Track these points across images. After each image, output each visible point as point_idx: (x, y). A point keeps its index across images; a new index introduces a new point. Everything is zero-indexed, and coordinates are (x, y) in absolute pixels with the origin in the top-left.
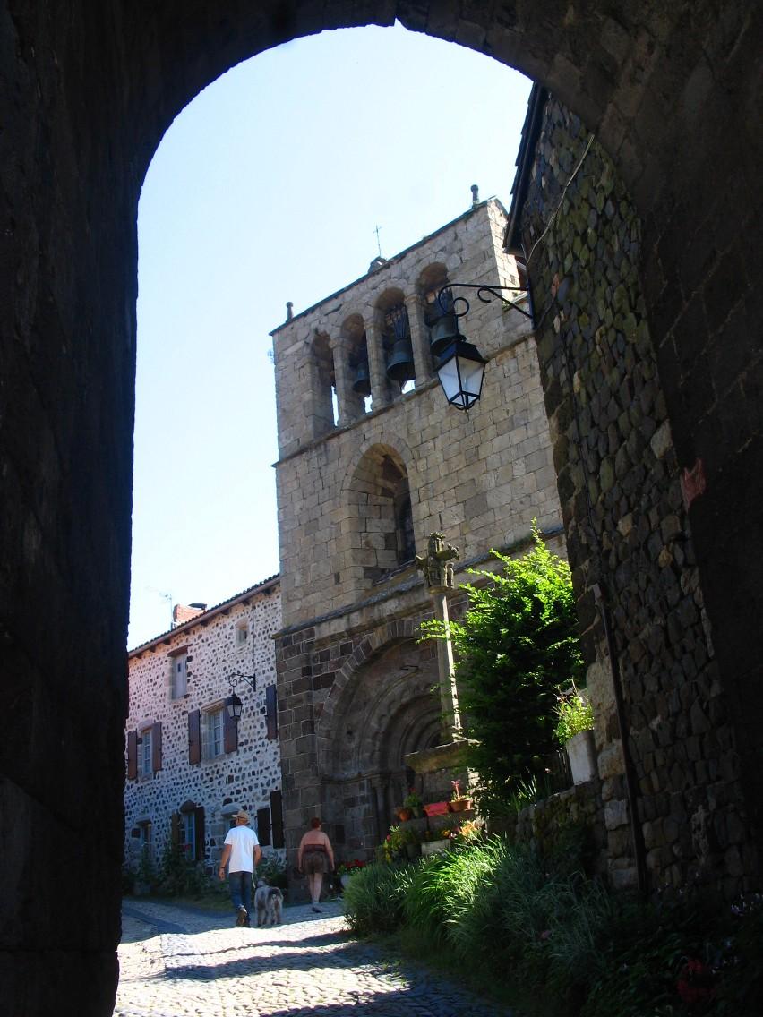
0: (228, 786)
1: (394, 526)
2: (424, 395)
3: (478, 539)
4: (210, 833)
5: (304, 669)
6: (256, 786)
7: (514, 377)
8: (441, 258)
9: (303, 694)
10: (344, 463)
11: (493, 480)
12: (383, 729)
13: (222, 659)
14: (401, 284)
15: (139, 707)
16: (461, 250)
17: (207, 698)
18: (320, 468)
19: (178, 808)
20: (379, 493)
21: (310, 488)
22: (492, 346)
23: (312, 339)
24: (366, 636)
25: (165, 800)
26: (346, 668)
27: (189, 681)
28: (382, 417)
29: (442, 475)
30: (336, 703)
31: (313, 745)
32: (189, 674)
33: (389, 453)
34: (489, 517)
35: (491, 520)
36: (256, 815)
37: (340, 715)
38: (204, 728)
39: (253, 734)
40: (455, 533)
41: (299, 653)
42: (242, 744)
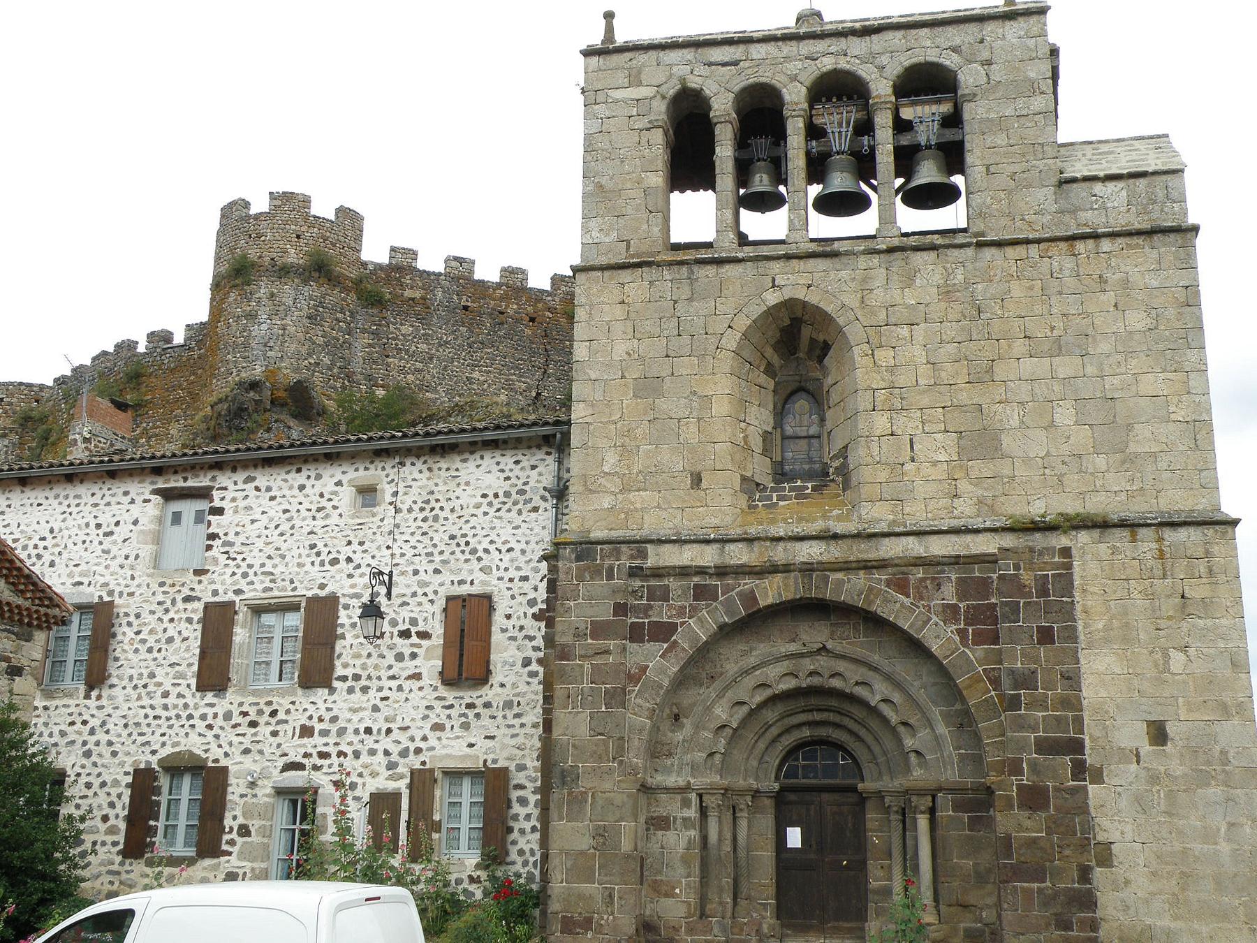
0: (297, 741)
2: (897, 255)
3: (980, 492)
4: (238, 812)
6: (372, 752)
7: (1071, 283)
9: (612, 644)
11: (1016, 417)
12: (735, 725)
13: (309, 529)
14: (865, 71)
15: (52, 564)
16: (989, 63)
17: (259, 587)
18: (676, 302)
19: (154, 760)
22: (1030, 224)
23: (672, 92)
24: (748, 583)
25: (114, 739)
26: (701, 621)
27: (209, 548)
28: (812, 262)
30: (675, 669)
32: (213, 537)
33: (806, 317)
35: (1006, 471)
36: (366, 798)
38: (240, 635)
39: (376, 667)
40: (940, 473)
41: (610, 576)
42: (344, 679)
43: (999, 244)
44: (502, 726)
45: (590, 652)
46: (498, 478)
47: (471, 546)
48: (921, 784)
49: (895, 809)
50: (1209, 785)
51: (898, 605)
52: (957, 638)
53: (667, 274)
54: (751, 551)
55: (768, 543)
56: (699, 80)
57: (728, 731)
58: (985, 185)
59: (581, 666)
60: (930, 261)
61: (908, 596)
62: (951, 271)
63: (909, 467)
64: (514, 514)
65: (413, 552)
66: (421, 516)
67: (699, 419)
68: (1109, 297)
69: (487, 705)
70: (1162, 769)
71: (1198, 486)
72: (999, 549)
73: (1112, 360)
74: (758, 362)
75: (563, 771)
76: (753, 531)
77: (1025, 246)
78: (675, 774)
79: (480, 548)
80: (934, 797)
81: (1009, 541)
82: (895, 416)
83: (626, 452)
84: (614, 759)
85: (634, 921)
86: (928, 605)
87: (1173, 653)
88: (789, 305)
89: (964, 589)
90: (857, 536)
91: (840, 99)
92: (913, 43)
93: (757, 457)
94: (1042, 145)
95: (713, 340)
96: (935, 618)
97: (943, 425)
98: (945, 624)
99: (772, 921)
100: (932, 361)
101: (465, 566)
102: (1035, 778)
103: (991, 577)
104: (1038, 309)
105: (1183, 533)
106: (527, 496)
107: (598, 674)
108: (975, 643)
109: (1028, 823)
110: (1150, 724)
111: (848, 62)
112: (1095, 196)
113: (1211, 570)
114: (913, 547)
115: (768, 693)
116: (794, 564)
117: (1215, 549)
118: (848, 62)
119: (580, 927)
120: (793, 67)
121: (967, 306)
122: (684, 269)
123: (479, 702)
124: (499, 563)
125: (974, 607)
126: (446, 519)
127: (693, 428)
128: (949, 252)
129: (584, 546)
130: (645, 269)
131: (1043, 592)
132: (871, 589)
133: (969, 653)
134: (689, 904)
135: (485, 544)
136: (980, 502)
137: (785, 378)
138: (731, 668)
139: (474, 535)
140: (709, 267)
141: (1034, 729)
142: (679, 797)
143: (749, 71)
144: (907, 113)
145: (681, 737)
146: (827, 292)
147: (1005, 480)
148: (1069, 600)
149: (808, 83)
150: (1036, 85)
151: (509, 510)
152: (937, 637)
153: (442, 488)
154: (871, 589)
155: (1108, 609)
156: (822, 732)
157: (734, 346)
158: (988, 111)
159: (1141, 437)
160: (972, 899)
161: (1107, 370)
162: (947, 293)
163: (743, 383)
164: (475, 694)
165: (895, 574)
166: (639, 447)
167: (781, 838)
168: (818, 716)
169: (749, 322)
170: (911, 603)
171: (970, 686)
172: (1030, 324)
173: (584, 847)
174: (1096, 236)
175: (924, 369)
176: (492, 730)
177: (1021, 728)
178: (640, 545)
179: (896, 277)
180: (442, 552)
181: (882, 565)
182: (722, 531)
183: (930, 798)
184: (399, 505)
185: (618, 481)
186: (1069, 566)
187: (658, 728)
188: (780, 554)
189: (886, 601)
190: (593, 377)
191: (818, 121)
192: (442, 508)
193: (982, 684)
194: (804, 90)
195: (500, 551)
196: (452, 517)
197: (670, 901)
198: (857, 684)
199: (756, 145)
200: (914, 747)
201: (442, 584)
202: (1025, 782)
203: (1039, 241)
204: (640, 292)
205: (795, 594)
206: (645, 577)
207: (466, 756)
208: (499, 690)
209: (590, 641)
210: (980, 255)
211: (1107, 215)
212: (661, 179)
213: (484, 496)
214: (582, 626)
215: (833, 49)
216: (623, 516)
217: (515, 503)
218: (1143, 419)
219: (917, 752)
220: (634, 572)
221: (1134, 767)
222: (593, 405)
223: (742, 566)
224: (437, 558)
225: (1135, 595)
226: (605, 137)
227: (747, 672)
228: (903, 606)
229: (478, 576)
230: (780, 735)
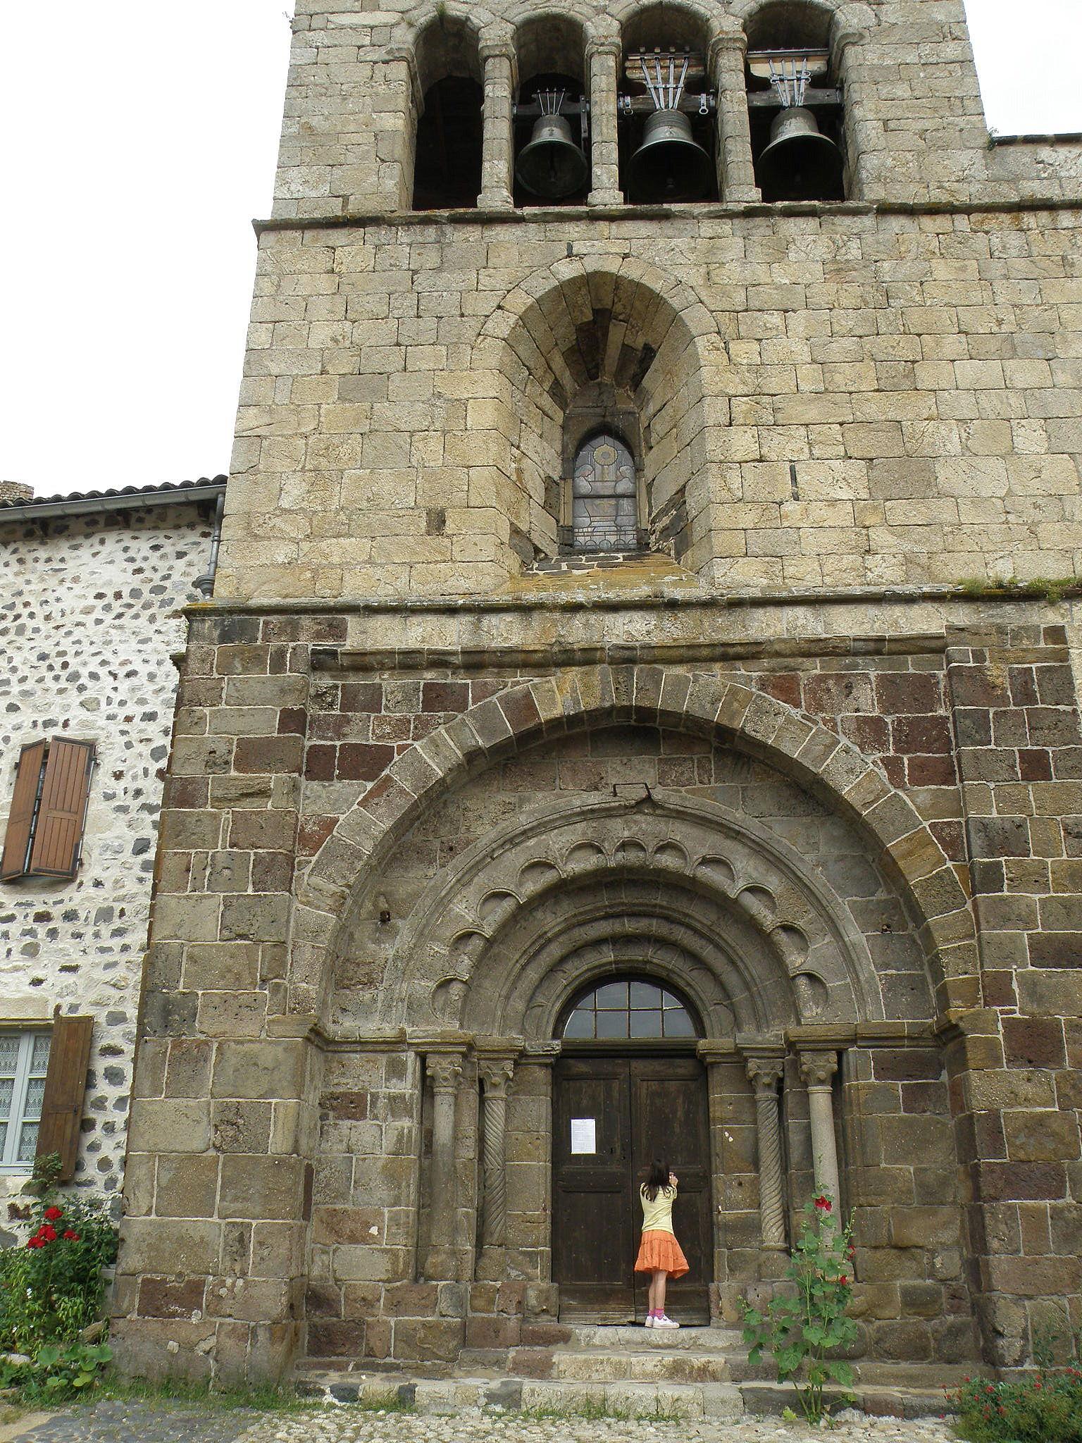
3: (907, 547)
7: (1021, 264)
9: (273, 779)
10: (497, 279)
11: (956, 439)
12: (488, 932)
18: (415, 272)
20: (547, 386)
23: (422, 20)
24: (519, 683)
30: (386, 825)
33: (618, 308)
34: (944, 511)
35: (948, 516)
40: (842, 515)
41: (278, 666)
43: (910, 211)
44: (92, 951)
45: (233, 793)
46: (124, 571)
47: (69, 670)
48: (820, 1031)
49: (766, 1080)
51: (781, 719)
52: (883, 773)
54: (528, 627)
55: (557, 615)
57: (476, 944)
59: (215, 817)
61: (797, 705)
62: (841, 244)
63: (789, 507)
64: (143, 621)
67: (444, 433)
69: (70, 916)
72: (948, 628)
74: (540, 373)
75: (167, 1002)
76: (531, 597)
77: (948, 216)
78: (377, 1017)
79: (84, 672)
80: (840, 1054)
81: (962, 615)
83: (318, 478)
85: (285, 1289)
86: (833, 720)
88: (591, 282)
89: (891, 691)
90: (709, 605)
93: (537, 510)
94: (962, 98)
95: (472, 325)
96: (844, 741)
98: (862, 750)
100: (819, 359)
101: (59, 700)
102: (1034, 1008)
103: (934, 676)
104: (976, 297)
106: (166, 596)
107: (242, 835)
108: (915, 781)
109: (1027, 1089)
112: (1042, 162)
114: (805, 623)
115: (549, 877)
116: (602, 649)
119: (178, 1301)
123: (57, 911)
124: (112, 694)
125: (911, 723)
126: (36, 630)
127: (435, 444)
128: (838, 220)
129: (236, 617)
131: (1026, 696)
132: (733, 692)
133: (905, 797)
134: (394, 1255)
135: (93, 666)
137: (579, 410)
138: (486, 833)
139: (77, 654)
140: (470, 228)
141: (1028, 923)
142: (383, 1059)
144: (760, 70)
145: (392, 952)
146: (652, 264)
147: (947, 529)
148: (1069, 708)
151: (136, 616)
152: (851, 771)
154: (733, 692)
156: (636, 954)
157: (504, 331)
160: (914, 1234)
162: (838, 270)
164: (51, 898)
165: (774, 670)
166: (342, 471)
167: (561, 1137)
168: (630, 926)
169: (530, 301)
171: (910, 853)
172: (965, 315)
173: (197, 1144)
176: (74, 956)
177: (1006, 921)
179: (758, 249)
180: (23, 680)
181: (751, 652)
183: (833, 1057)
186: (1064, 656)
187: (351, 935)
188: (577, 632)
189: (760, 712)
190: (275, 371)
191: (633, 75)
193: (930, 850)
194: (616, 25)
195: (115, 676)
196: (46, 628)
197: (360, 1250)
198: (705, 861)
200: (806, 968)
201: (17, 728)
202: (1017, 1015)
203: (968, 210)
204: (359, 258)
205: (603, 699)
207: (27, 1001)
208: (92, 891)
209: (233, 773)
210: (883, 226)
211: (1061, 187)
212: (401, 122)
213: (100, 596)
214: (221, 749)
216: (308, 575)
217: (146, 606)
219: (811, 977)
220: (320, 662)
222: (271, 411)
226: (321, 71)
227: (512, 841)
228: (789, 720)
229: (78, 715)
230: (563, 959)
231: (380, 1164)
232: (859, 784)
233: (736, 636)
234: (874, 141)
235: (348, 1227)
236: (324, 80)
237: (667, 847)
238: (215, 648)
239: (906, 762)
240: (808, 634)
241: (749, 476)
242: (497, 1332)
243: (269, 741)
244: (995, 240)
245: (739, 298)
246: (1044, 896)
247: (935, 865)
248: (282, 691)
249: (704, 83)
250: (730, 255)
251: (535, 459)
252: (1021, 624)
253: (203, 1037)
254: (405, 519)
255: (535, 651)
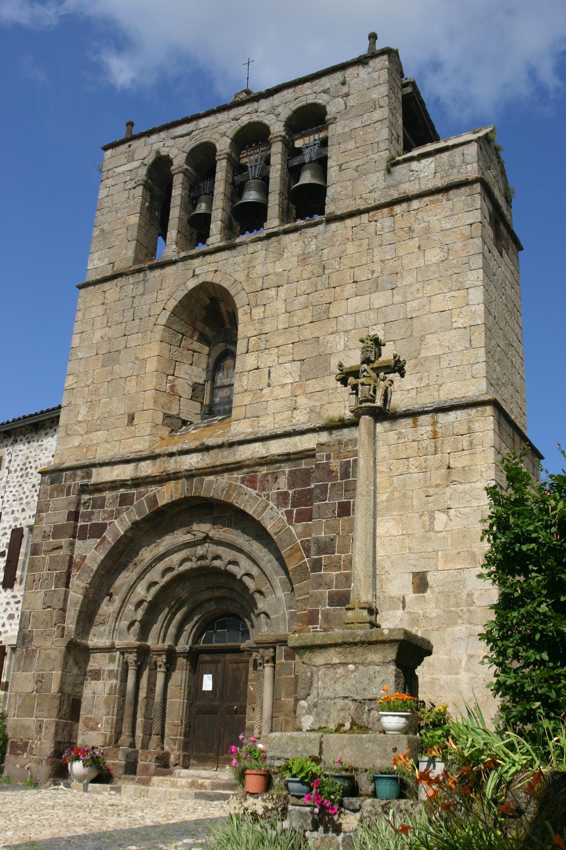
1: (204, 377)
2: (273, 239)
3: (312, 403)
5: (70, 513)
7: (388, 237)
8: (322, 100)
9: (64, 541)
10: (163, 296)
12: (149, 599)
14: (268, 120)
16: (347, 95)
18: (134, 297)
21: (117, 317)
22: (366, 200)
23: (151, 161)
24: (153, 490)
29: (280, 327)
30: (102, 557)
31: (65, 600)
33: (218, 296)
37: (103, 573)
40: (286, 392)
41: (68, 494)
45: (51, 548)
50: (455, 624)
51: (247, 496)
52: (285, 518)
53: (131, 279)
54: (154, 465)
55: (165, 458)
56: (167, 150)
57: (145, 605)
58: (337, 179)
60: (294, 239)
61: (255, 489)
62: (307, 243)
63: (266, 391)
65: (13, 498)
66: (20, 474)
67: (137, 376)
68: (415, 242)
70: (421, 612)
71: (469, 377)
73: (413, 288)
76: (158, 451)
78: (105, 637)
80: (275, 648)
81: (324, 437)
82: (260, 354)
83: (92, 405)
84: (55, 624)
86: (268, 495)
87: (439, 515)
88: (203, 287)
90: (221, 446)
91: (257, 144)
92: (300, 94)
94: (378, 143)
95: (153, 319)
96: (271, 504)
97: (291, 356)
98: (278, 507)
99: (178, 753)
105: (452, 415)
108: (298, 521)
110: (415, 574)
111: (258, 116)
112: (412, 171)
113: (471, 443)
116: (180, 472)
117: (476, 426)
118: (258, 116)
120: (223, 128)
121: (316, 266)
122: (141, 275)
125: (300, 493)
126: (32, 474)
127: (134, 383)
130: (119, 279)
132: (230, 485)
136: (312, 411)
141: (329, 586)
142: (108, 655)
143: (197, 137)
144: (298, 144)
145: (112, 610)
146: (226, 273)
147: (330, 391)
149: (231, 136)
150: (377, 103)
152: (272, 518)
153: (33, 454)
154: (230, 485)
155: (392, 484)
158: (343, 128)
159: (430, 345)
161: (409, 297)
162: (304, 259)
163: (174, 348)
165: (248, 473)
166: (100, 400)
168: (217, 593)
170: (257, 494)
171: (290, 555)
173: (30, 690)
174: (407, 199)
175: (283, 318)
177: (320, 585)
178: (87, 468)
181: (238, 466)
182: (140, 454)
184: (11, 468)
185: (84, 425)
188: (172, 465)
189: (239, 494)
190: (80, 357)
192: (31, 467)
193: (299, 553)
194: (229, 141)
197: (94, 733)
198: (230, 563)
199: (204, 185)
203: (367, 211)
206: (91, 492)
209: (51, 540)
214: (48, 530)
215: (249, 110)
216: (85, 450)
218: (433, 330)
220: (84, 489)
221: (400, 612)
222: (77, 376)
223: (148, 477)
224: (25, 501)
225: (413, 470)
231: (103, 698)
232: (274, 524)
233: (231, 460)
234: (334, 178)
235: (91, 724)
236: (109, 204)
237: (217, 557)
238: (49, 487)
239: (295, 512)
240: (259, 455)
241: (251, 378)
242: (147, 770)
243: (63, 525)
244: (379, 225)
245: (259, 284)
246: (338, 573)
247: (300, 560)
248: (69, 504)
249: (268, 161)
250: (259, 261)
251: (186, 377)
252: (350, 438)
253: (34, 648)
254: (120, 420)
255: (156, 476)
